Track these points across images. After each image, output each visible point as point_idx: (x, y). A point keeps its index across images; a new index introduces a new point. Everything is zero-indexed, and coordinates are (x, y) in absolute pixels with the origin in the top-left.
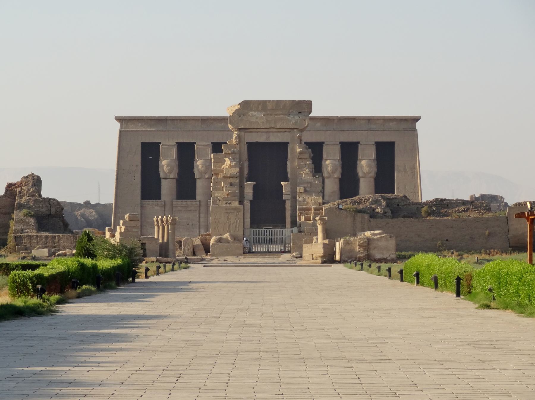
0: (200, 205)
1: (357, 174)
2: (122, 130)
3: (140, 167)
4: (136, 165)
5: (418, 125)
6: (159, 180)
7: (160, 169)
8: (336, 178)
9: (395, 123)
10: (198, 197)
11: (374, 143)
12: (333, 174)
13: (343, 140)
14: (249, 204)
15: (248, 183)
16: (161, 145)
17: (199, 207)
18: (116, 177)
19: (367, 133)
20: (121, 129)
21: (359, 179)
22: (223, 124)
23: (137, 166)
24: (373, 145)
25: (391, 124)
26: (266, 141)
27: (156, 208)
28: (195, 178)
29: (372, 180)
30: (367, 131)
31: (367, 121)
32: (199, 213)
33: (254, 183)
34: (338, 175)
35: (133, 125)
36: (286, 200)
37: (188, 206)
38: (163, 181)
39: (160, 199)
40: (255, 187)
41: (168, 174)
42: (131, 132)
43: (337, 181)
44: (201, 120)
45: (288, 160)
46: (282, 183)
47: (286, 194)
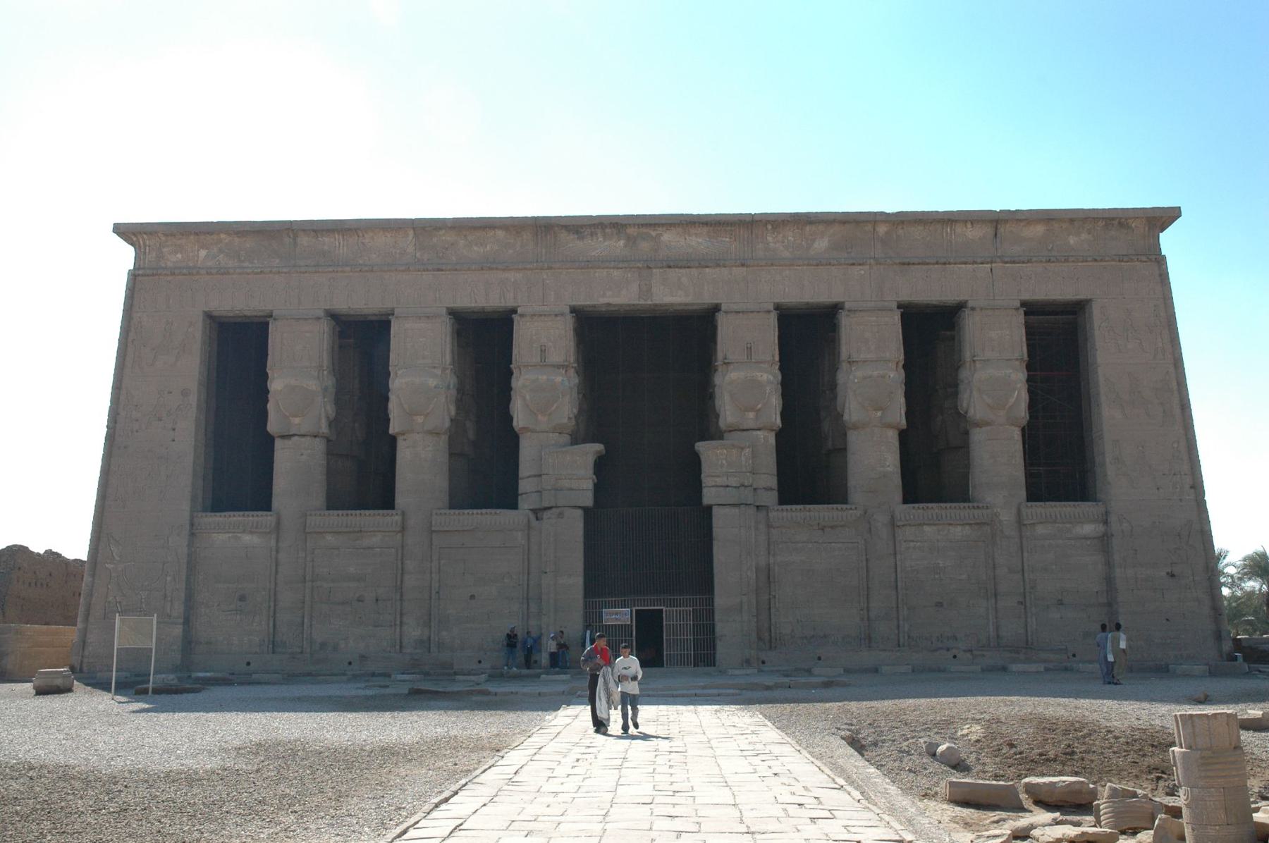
0: (403, 529)
1: (961, 417)
2: (140, 272)
3: (193, 399)
4: (182, 392)
5: (1169, 241)
6: (267, 443)
7: (270, 406)
8: (889, 426)
9: (1084, 236)
10: (400, 500)
11: (1019, 305)
12: (879, 414)
13: (906, 296)
14: (581, 525)
15: (576, 447)
16: (271, 321)
17: (400, 534)
18: (106, 430)
19: (991, 270)
20: (139, 269)
21: (967, 433)
22: (488, 248)
23: (185, 393)
24: (1017, 309)
25: (1072, 240)
26: (642, 302)
27: (247, 538)
28: (391, 431)
29: (1017, 434)
30: (991, 262)
31: (988, 230)
32: (400, 557)
33: (599, 447)
34: (897, 412)
35: (179, 256)
36: (715, 510)
37: (361, 531)
38: (278, 444)
39: (268, 507)
40: (601, 466)
41: (297, 420)
42: (170, 278)
43: (893, 436)
44: (411, 233)
45: (716, 370)
46: (700, 446)
47: (713, 484)
